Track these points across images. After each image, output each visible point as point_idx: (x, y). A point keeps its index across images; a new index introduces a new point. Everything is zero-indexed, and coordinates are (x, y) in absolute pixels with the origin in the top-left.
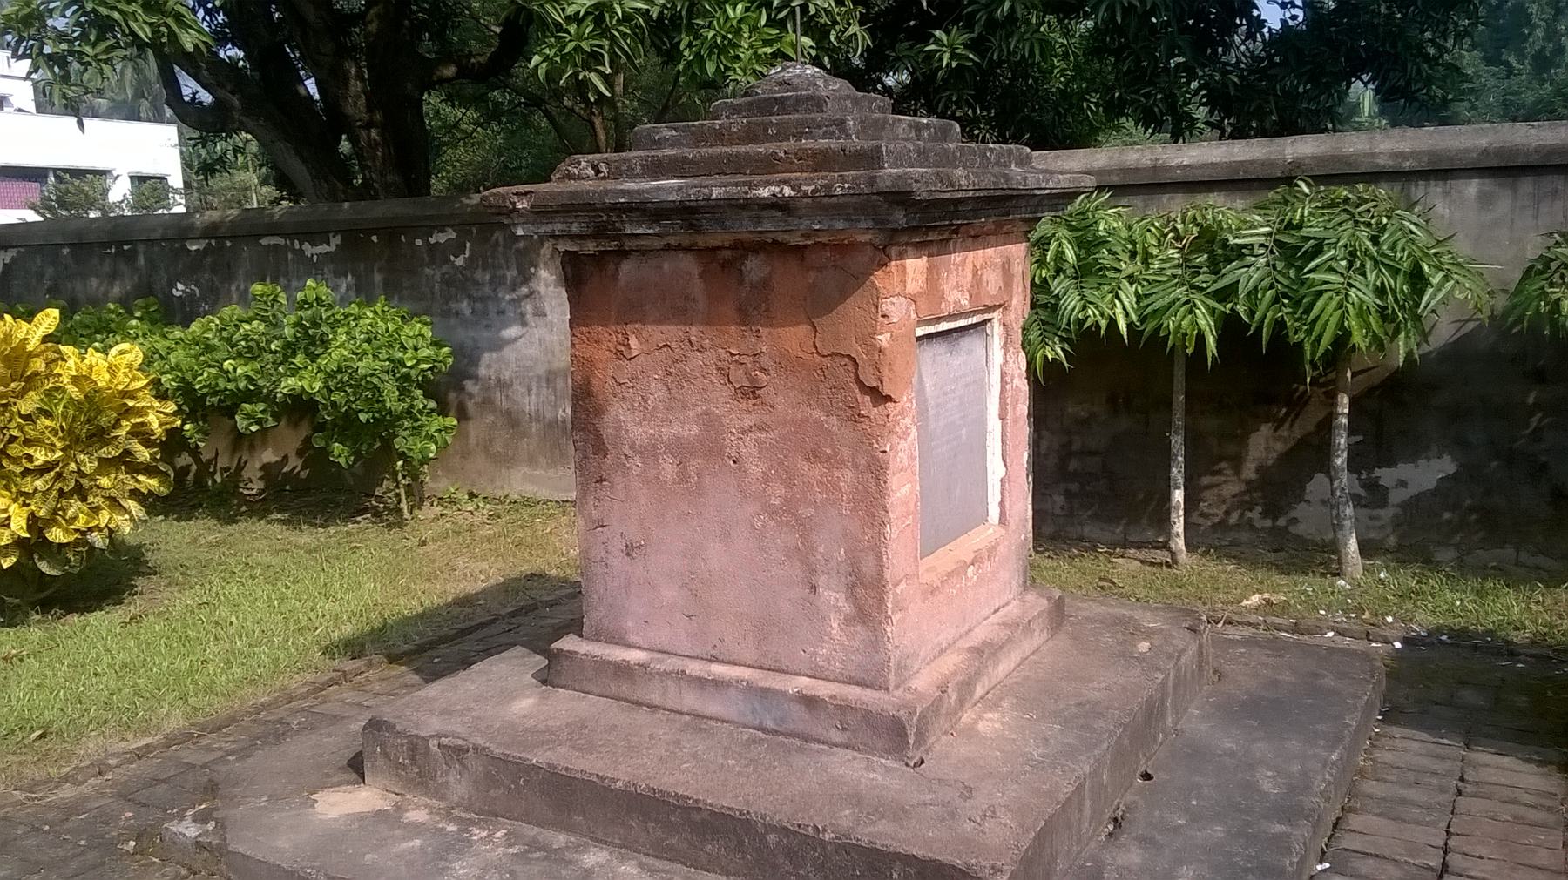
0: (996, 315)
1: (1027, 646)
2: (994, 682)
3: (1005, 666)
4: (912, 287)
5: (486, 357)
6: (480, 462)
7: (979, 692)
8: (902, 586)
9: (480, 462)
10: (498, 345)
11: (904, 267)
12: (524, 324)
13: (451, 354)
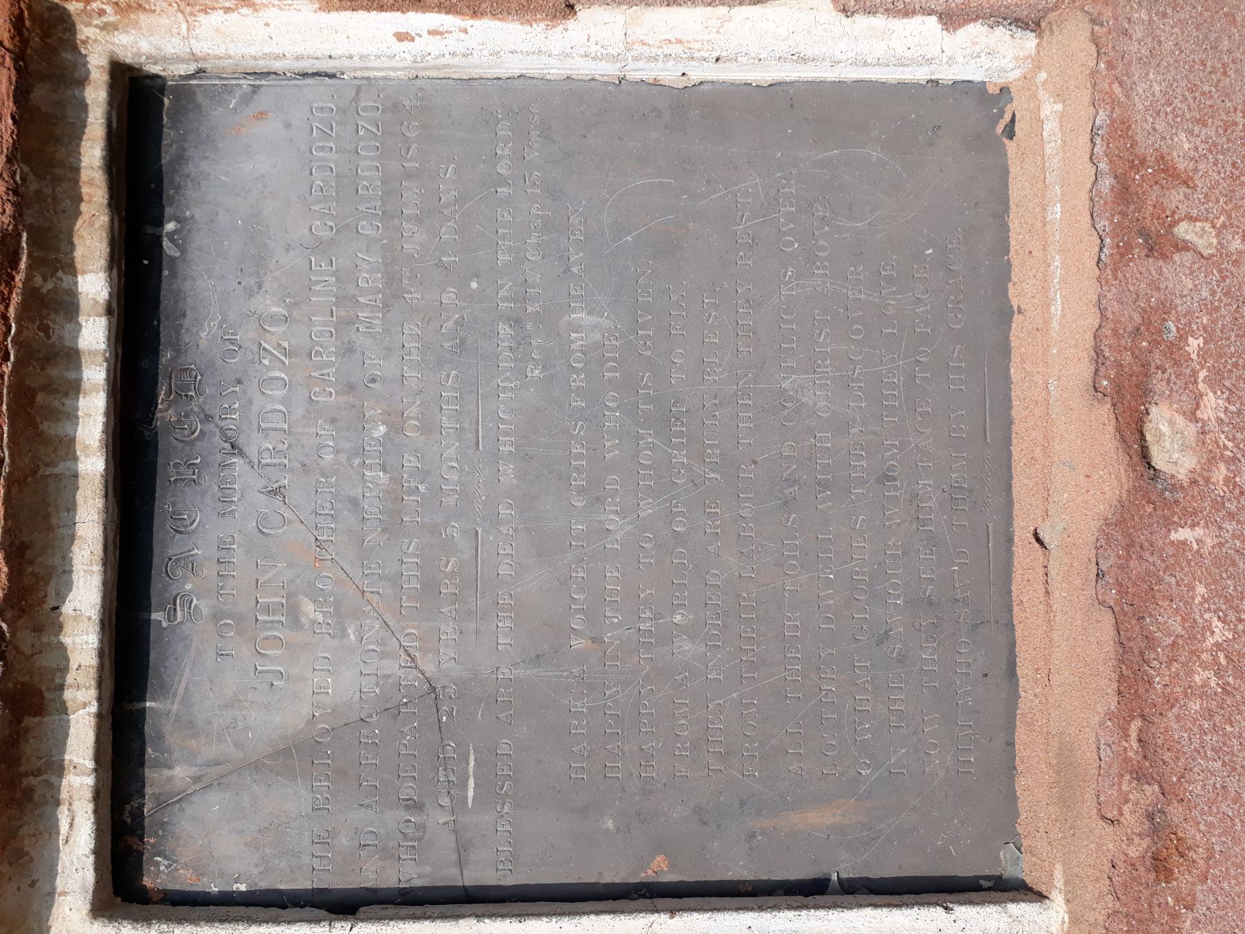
0: (102, 43)
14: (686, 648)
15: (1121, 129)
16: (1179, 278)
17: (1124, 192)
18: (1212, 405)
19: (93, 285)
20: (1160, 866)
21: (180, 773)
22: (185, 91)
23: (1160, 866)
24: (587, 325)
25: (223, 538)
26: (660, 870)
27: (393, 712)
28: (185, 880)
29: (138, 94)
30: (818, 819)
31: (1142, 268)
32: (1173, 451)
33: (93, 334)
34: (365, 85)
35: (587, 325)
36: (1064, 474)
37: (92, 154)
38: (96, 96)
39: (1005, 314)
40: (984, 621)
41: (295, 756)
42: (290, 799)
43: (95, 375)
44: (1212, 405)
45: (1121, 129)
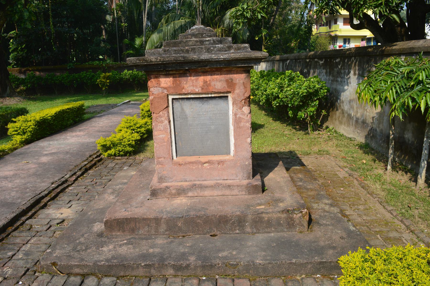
0: (229, 95)
1: (227, 192)
2: (201, 195)
3: (207, 193)
4: (163, 85)
5: (342, 93)
6: (337, 122)
7: (190, 194)
8: (162, 159)
9: (337, 122)
10: (344, 91)
11: (159, 81)
12: (348, 86)
13: (326, 92)
14: (191, 135)
15: (226, 161)
16: (217, 165)
17: (222, 162)
18: (208, 167)
19: (213, 95)
20: (179, 164)
21: (181, 102)
22: (227, 99)
23: (179, 164)
24: (213, 127)
25: (197, 104)
26: (176, 133)
27: (186, 115)
28: (174, 103)
29: (227, 97)
30: (180, 143)
31: (217, 163)
32: (205, 165)
33: (210, 96)
34: (228, 111)
35: (213, 127)
36: (203, 159)
37: (222, 95)
38: (226, 95)
39: (215, 155)
40: (194, 154)
41: (182, 109)
42: (179, 109)
43: (207, 96)
44: (208, 167)
45: (226, 161)
